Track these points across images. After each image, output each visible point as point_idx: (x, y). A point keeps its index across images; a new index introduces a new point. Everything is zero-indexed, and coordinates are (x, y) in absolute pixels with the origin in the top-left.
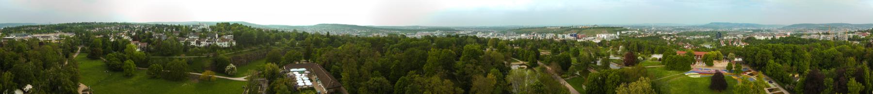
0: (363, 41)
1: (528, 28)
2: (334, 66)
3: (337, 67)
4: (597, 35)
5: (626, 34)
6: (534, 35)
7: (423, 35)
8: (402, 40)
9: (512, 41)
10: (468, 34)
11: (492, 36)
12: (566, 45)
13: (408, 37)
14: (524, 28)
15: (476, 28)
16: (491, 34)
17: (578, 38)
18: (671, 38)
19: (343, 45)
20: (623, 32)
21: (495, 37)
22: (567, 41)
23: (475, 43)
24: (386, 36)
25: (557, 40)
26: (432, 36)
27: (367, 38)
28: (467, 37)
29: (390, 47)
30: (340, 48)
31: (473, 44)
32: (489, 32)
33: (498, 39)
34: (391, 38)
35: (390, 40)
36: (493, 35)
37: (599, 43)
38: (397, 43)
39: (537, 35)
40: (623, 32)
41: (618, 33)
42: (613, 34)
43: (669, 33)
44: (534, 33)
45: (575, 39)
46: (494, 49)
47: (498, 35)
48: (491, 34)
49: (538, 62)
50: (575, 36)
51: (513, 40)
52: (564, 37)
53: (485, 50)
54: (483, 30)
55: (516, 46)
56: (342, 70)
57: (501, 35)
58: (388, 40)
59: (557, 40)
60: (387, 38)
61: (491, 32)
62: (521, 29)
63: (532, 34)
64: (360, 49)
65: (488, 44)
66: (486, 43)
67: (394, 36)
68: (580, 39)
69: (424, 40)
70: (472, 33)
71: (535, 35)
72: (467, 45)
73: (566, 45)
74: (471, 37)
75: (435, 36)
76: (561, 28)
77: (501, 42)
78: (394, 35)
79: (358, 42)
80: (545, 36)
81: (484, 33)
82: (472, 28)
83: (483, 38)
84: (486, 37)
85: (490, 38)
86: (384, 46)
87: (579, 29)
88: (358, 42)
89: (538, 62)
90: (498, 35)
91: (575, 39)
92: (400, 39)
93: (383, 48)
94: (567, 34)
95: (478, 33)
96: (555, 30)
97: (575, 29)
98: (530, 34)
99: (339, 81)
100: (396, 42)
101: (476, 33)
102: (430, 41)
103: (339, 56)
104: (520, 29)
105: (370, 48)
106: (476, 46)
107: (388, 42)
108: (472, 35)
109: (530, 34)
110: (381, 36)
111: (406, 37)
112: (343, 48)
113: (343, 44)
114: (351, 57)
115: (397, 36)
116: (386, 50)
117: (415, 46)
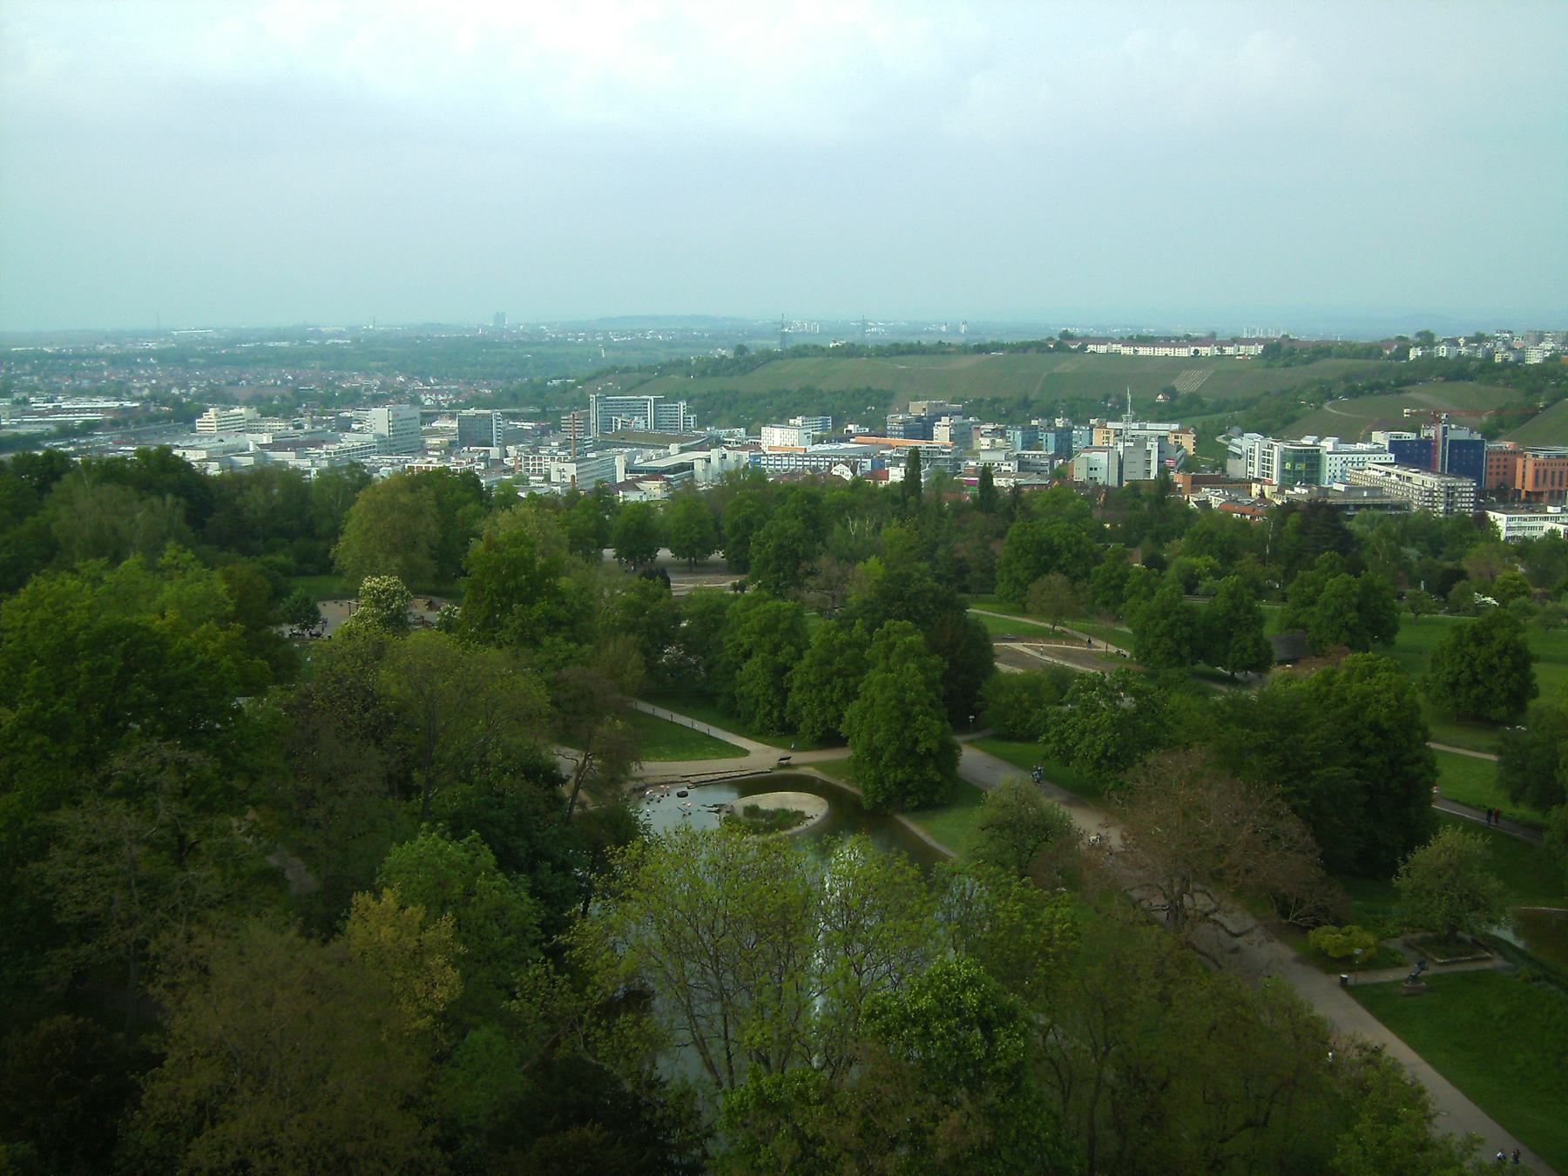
1: (850, 351)
6: (923, 429)
9: (645, 509)
10: (66, 432)
11: (387, 446)
12: (1356, 569)
14: (801, 352)
15: (179, 357)
16: (379, 420)
17: (1507, 497)
21: (433, 462)
22: (1352, 525)
23: (154, 549)
25: (1216, 499)
28: (52, 469)
31: (132, 562)
32: (354, 399)
33: (470, 480)
36: (403, 440)
39: (962, 438)
44: (918, 409)
45: (1466, 505)
46: (419, 608)
47: (472, 435)
48: (379, 420)
49: (972, 758)
50: (1464, 459)
51: (653, 490)
52: (1307, 468)
53: (308, 616)
54: (274, 381)
55: (693, 555)
57: (516, 437)
59: (1216, 499)
61: (377, 400)
62: (768, 357)
63: (895, 419)
65: (346, 550)
66: (309, 531)
68: (1532, 502)
70: (119, 422)
71: (942, 433)
72: (40, 584)
73: (1356, 569)
74: (112, 472)
76: (1278, 351)
77: (502, 524)
80: (1065, 449)
81: (286, 411)
82: (117, 361)
83: (264, 476)
84: (310, 464)
85: (366, 480)
87: (1516, 372)
89: (972, 758)
90: (472, 435)
91: (1466, 505)
94: (1349, 433)
95: (210, 419)
96: (1187, 384)
97: (1457, 371)
98: (877, 428)
101: (186, 416)
104: (745, 361)
106: (169, 591)
108: (128, 451)
109: (877, 428)
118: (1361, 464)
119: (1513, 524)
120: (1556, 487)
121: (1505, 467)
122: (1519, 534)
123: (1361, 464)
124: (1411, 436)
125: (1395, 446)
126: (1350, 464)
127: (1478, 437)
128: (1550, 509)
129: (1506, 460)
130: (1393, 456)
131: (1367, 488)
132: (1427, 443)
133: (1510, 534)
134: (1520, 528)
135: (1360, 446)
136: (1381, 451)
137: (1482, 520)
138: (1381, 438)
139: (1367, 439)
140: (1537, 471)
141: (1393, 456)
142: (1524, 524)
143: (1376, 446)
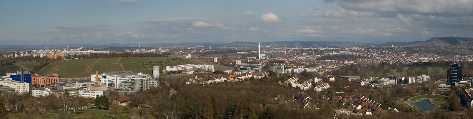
4: (93, 78)
5: (179, 72)
18: (314, 85)
20: (169, 68)
37: (98, 99)
40: (169, 68)
41: (156, 72)
42: (140, 74)
43: (308, 70)
45: (27, 89)
118: (4, 81)
119: (38, 92)
120: (47, 84)
121: (36, 80)
122: (39, 94)
123: (4, 81)
124: (16, 74)
125: (12, 77)
126: (2, 81)
127: (30, 73)
128: (46, 88)
129: (36, 78)
130: (11, 78)
131: (6, 86)
132: (19, 76)
133: (37, 94)
134: (39, 93)
135: (4, 77)
136: (8, 78)
137: (30, 93)
138: (9, 75)
139: (6, 75)
140: (43, 80)
141: (11, 78)
142: (40, 92)
143: (7, 77)
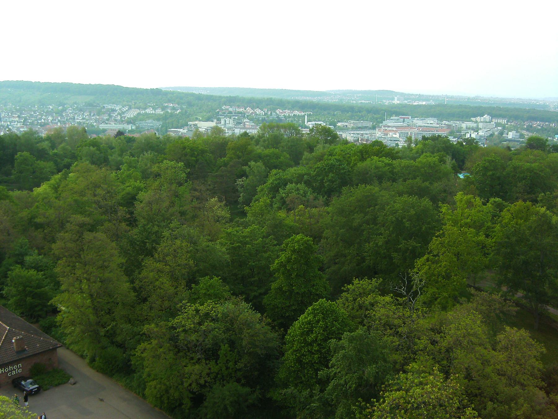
0: (148, 155)
2: (17, 271)
3: (32, 272)
7: (415, 134)
8: (319, 149)
13: (346, 142)
19: (58, 176)
24: (254, 132)
26: (453, 140)
27: (168, 139)
29: (270, 180)
30: (43, 189)
34: (276, 141)
35: (267, 152)
38: (297, 164)
56: (58, 284)
58: (259, 150)
60: (258, 140)
64: (139, 189)
67: (286, 135)
69: (420, 153)
75: (470, 141)
78: (285, 127)
79: (126, 158)
86: (243, 174)
88: (126, 158)
92: (311, 149)
93: (240, 182)
99: (48, 329)
100: (296, 159)
102: (448, 159)
103: (38, 226)
105: (180, 184)
107: (259, 157)
110: (228, 134)
111: (335, 137)
112: (56, 188)
113: (59, 171)
114: (92, 228)
115: (298, 132)
116: (252, 193)
117: (380, 178)
